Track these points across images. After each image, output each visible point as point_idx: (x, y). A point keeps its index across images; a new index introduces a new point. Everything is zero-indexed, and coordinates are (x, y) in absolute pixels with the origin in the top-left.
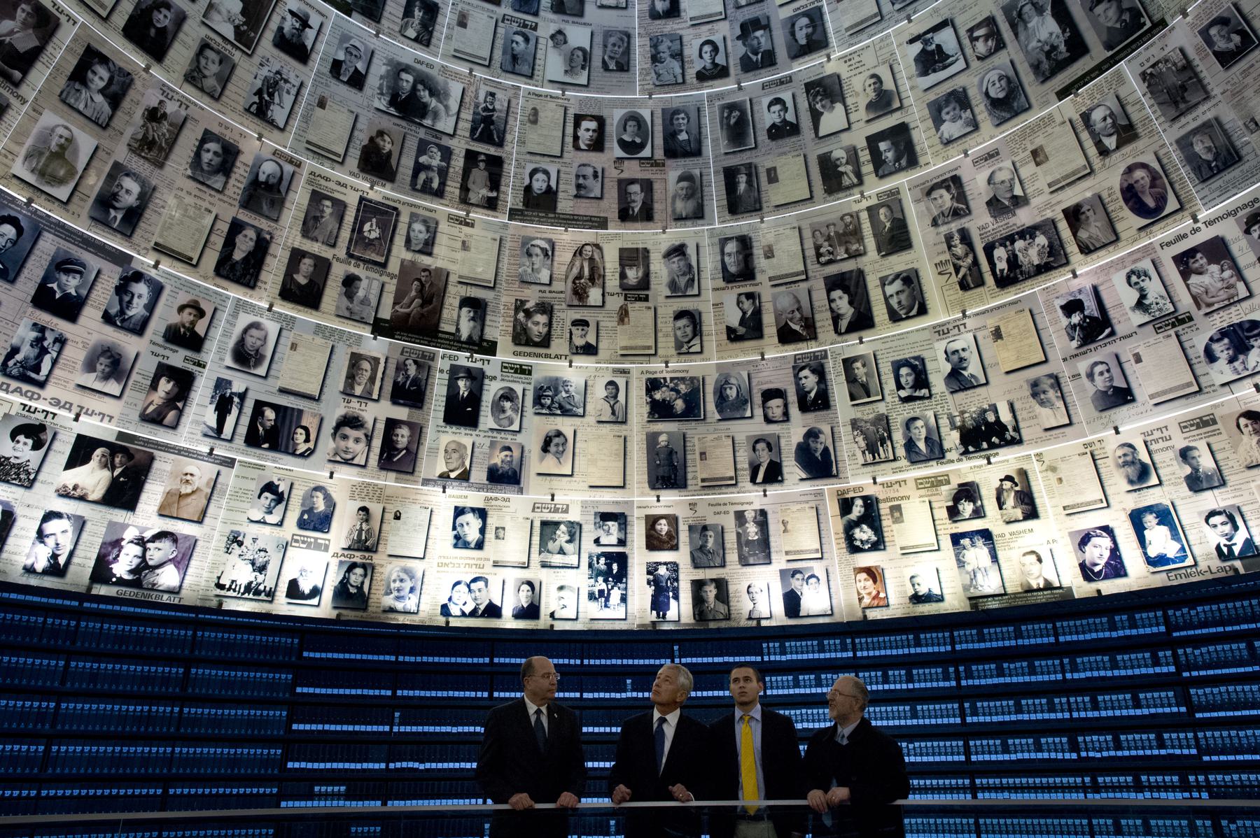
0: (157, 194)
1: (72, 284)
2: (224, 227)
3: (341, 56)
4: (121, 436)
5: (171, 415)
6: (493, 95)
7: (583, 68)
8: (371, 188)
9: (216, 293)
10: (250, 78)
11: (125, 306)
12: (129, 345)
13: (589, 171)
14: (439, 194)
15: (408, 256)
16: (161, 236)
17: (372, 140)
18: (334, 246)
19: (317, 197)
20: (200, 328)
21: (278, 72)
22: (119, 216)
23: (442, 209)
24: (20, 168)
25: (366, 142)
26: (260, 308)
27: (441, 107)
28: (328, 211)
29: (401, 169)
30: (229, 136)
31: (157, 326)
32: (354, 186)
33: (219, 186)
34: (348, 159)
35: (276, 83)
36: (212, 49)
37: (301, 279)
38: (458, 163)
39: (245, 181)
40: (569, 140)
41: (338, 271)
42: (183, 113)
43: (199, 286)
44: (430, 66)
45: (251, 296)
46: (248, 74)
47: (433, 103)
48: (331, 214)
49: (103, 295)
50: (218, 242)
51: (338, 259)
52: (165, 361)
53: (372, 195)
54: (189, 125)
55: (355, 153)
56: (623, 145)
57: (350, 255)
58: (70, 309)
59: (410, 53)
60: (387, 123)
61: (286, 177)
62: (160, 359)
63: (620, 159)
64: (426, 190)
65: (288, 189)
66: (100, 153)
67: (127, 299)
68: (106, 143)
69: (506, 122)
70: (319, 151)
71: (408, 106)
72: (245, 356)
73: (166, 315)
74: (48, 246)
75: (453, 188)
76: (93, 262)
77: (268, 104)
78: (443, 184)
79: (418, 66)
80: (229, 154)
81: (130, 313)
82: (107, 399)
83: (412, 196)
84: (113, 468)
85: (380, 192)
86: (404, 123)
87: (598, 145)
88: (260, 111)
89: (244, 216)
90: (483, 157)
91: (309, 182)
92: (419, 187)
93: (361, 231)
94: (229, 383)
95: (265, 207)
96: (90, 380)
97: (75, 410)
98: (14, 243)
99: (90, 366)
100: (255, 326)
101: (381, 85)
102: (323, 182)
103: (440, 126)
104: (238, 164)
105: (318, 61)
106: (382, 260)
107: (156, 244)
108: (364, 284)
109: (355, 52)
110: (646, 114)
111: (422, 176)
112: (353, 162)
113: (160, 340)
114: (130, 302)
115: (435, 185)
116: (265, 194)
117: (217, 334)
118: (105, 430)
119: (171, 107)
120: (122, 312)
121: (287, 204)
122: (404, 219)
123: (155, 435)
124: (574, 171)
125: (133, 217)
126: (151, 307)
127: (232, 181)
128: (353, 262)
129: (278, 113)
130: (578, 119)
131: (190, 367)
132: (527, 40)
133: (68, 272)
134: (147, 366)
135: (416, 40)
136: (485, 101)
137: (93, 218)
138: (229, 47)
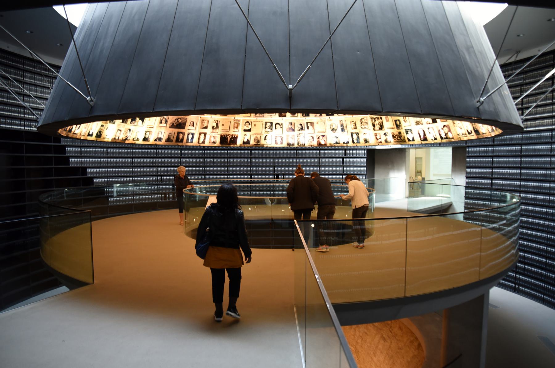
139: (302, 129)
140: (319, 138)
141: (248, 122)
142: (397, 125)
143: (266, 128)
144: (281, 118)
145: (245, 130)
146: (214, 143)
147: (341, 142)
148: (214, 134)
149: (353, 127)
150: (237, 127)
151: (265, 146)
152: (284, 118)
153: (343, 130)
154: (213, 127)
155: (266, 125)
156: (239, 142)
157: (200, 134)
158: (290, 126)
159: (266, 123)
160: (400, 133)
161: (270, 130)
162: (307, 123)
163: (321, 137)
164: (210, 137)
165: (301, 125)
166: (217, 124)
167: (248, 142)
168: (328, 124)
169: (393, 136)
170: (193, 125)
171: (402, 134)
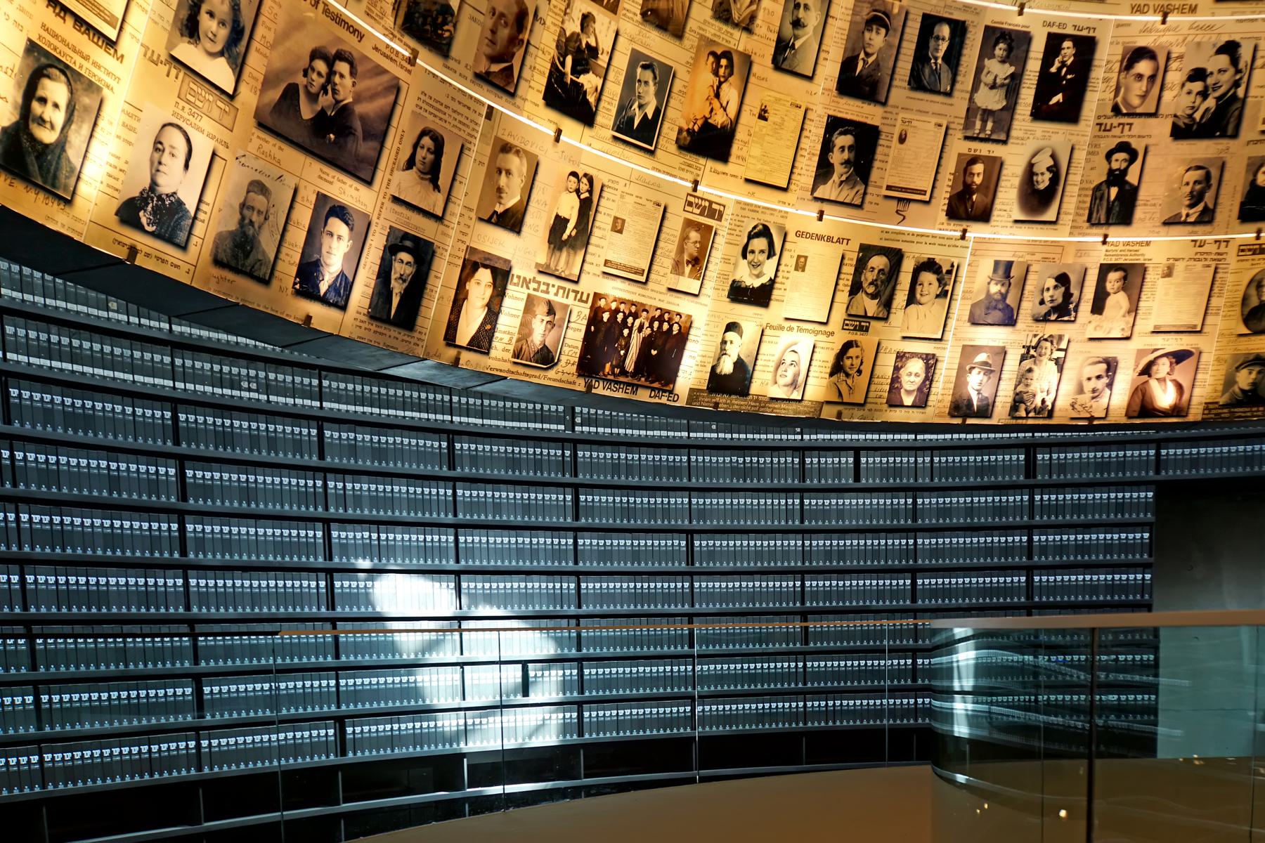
139: (1063, 310)
140: (1147, 371)
141: (765, 232)
143: (856, 288)
144: (953, 230)
145: (738, 293)
146: (546, 358)
148: (554, 292)
150: (696, 261)
152: (977, 231)
154: (557, 235)
155: (861, 265)
156: (691, 373)
157: (470, 267)
158: (995, 289)
159: (867, 251)
161: (872, 307)
162: (1105, 269)
165: (1063, 279)
166: (586, 207)
167: (743, 373)
170: (432, 174)
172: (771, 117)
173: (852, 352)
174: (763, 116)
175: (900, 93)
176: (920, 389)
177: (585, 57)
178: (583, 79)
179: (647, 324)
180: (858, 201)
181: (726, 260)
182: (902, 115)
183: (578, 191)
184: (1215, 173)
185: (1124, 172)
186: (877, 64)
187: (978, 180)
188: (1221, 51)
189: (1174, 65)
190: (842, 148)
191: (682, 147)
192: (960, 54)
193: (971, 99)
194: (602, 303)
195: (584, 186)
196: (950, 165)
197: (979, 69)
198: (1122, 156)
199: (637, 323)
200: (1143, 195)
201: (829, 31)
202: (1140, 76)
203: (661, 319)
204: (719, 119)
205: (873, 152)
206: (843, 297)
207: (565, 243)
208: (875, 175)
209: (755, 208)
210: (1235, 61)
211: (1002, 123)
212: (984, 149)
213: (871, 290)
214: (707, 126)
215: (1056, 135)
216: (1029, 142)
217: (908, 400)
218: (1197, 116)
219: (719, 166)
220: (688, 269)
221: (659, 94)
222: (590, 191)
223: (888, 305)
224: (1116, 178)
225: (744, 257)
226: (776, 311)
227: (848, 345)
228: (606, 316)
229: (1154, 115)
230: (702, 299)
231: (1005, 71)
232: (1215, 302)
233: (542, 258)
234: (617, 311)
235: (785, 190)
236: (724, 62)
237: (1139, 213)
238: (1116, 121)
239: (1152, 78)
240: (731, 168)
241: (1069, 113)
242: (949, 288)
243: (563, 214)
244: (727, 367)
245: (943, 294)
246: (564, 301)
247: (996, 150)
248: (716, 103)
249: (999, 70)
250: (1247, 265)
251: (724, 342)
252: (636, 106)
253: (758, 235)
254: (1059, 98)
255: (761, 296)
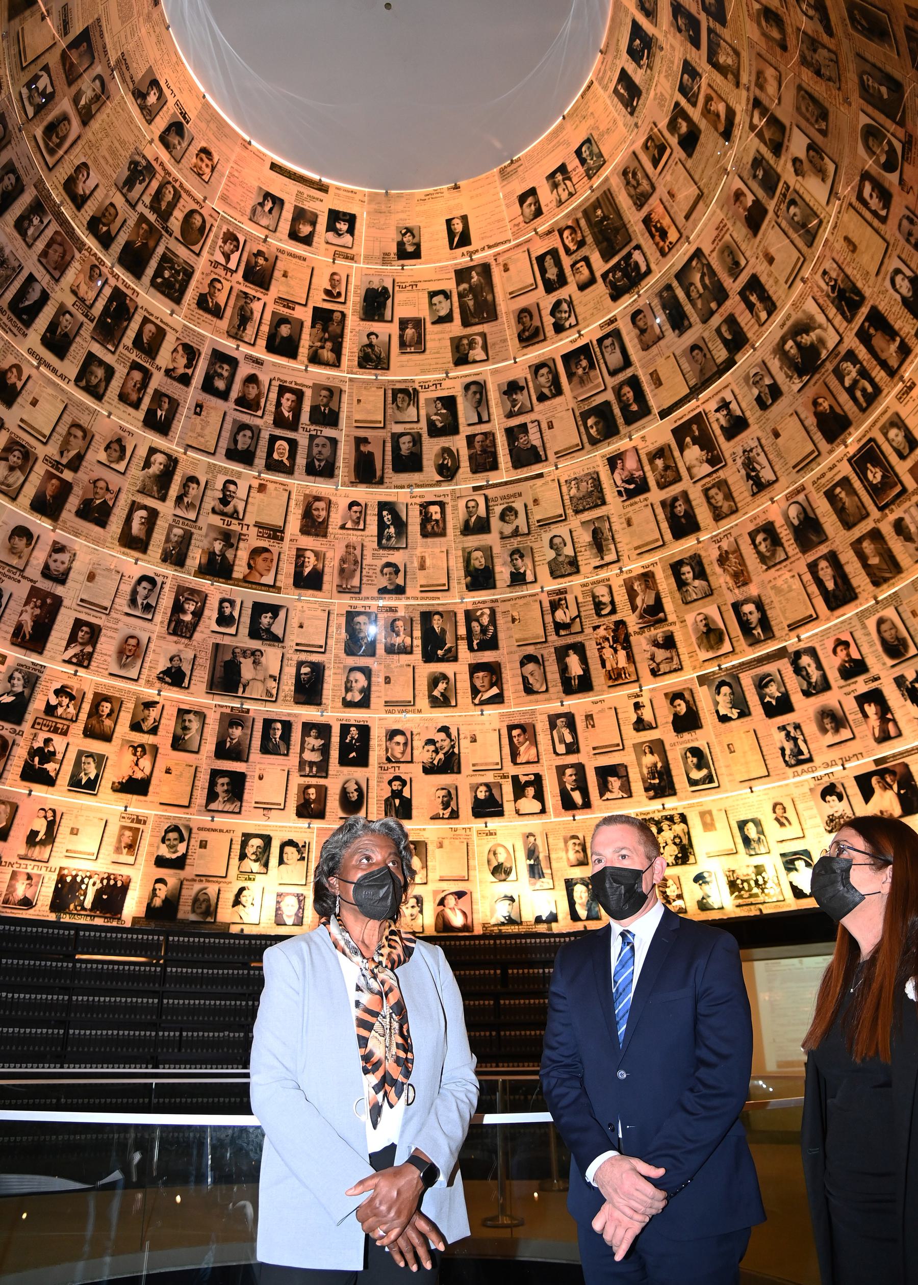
0: (763, 598)
1: (773, 690)
2: (808, 577)
3: (756, 392)
4: (877, 762)
5: (891, 726)
6: (825, 273)
7: (823, 159)
8: (846, 446)
9: (842, 622)
10: (738, 475)
11: (807, 677)
12: (829, 699)
13: (905, 223)
14: (878, 391)
15: (909, 463)
16: (786, 619)
17: (816, 414)
18: (868, 515)
19: (830, 495)
20: (855, 655)
21: (744, 451)
22: (759, 630)
23: (888, 402)
24: (704, 655)
25: (815, 421)
26: (872, 606)
27: (818, 331)
28: (843, 495)
29: (846, 408)
30: (760, 522)
31: (833, 676)
32: (837, 460)
33: (783, 557)
34: (819, 446)
35: (749, 458)
36: (710, 489)
37: (874, 561)
38: (862, 353)
39: (791, 536)
40: (876, 223)
41: (887, 529)
42: (732, 539)
43: (829, 628)
44: (789, 316)
45: (861, 605)
46: (733, 474)
47: (813, 335)
48: (847, 495)
49: (794, 684)
50: (813, 589)
51: (878, 521)
52: (857, 694)
53: (852, 450)
54: (740, 542)
55: (818, 436)
56: (889, 166)
57: (881, 509)
58: (783, 706)
59: (774, 329)
60: (810, 392)
61: (805, 504)
62: (853, 695)
63: (901, 181)
64: (872, 398)
65: (813, 510)
66: (723, 608)
67: (804, 673)
68: (720, 601)
69: (847, 276)
70: (803, 465)
71: (806, 362)
72: (895, 649)
73: (832, 664)
74: (747, 680)
75: (879, 375)
76: (770, 668)
77: (757, 476)
78: (872, 381)
79: (786, 328)
80: (769, 530)
81: (813, 680)
82: (849, 743)
83: (871, 415)
84: (891, 787)
85: (853, 441)
86: (817, 376)
87: (885, 196)
88: (759, 486)
89: (811, 557)
90: (867, 324)
91: (818, 490)
92: (864, 405)
93: (870, 483)
94: (902, 676)
95: (814, 538)
96: (830, 738)
97: (840, 762)
98: (733, 693)
99: (824, 731)
100: (881, 622)
101: (786, 373)
102: (823, 481)
103: (831, 345)
104: (779, 531)
105: (752, 414)
106: (899, 488)
107: (789, 626)
108: (908, 520)
109: (757, 378)
110: (864, 120)
111: (858, 394)
112: (823, 445)
113: (842, 682)
114: (808, 674)
115: (870, 389)
116: (808, 530)
117: (865, 650)
118: (865, 764)
119: (725, 545)
120: (809, 684)
121: (822, 520)
122: (881, 439)
123: (894, 748)
124: (902, 241)
125: (765, 623)
126: (820, 667)
127: (786, 545)
128: (887, 511)
129: (767, 475)
130: (860, 198)
131: (873, 685)
132: (793, 202)
133: (766, 685)
134: (851, 706)
135: (769, 314)
136: (827, 284)
137: (750, 645)
138: (714, 476)
140: (442, 902)
142: (747, 841)
143: (243, 856)
144: (303, 823)
145: (160, 862)
147: (528, 916)
149: (573, 856)
151: (234, 929)
153: (535, 871)
154: (32, 839)
155: (244, 844)
156: (133, 906)
159: (247, 837)
160: (759, 870)
161: (256, 867)
163: (451, 901)
164: (14, 875)
166: (52, 826)
168: (480, 848)
169: (733, 885)
171: (769, 874)
172: (174, 772)
173: (245, 893)
174: (168, 771)
175: (255, 755)
176: (296, 915)
177: (48, 757)
178: (45, 766)
179: (98, 881)
180: (237, 810)
181: (151, 845)
182: (258, 766)
183: (45, 817)
184: (453, 792)
185: (401, 791)
186: (239, 743)
187: (313, 797)
188: (440, 730)
189: (415, 738)
190: (223, 785)
191: (115, 790)
192: (289, 736)
193: (300, 757)
194: (66, 872)
195: (50, 814)
196: (294, 790)
197: (303, 742)
198: (397, 783)
199: (92, 881)
200: (414, 803)
201: (205, 730)
202: (398, 743)
203: (108, 879)
204: (139, 775)
205: (243, 785)
206: (235, 861)
207: (38, 843)
208: (246, 796)
209: (168, 818)
210: (449, 735)
211: (322, 768)
212: (313, 781)
213: (254, 857)
214: (131, 779)
215: (358, 773)
216: (339, 777)
217: (290, 921)
218: (436, 762)
219: (142, 798)
220: (125, 851)
221: (98, 767)
222: (54, 816)
223: (266, 865)
224: (397, 794)
225: (163, 841)
226: (189, 872)
227: (242, 890)
228: (69, 879)
229: (412, 762)
230: (136, 866)
231: (318, 743)
232: (471, 862)
233: (22, 852)
234: (77, 875)
235: (188, 807)
236: (139, 749)
237: (414, 813)
238: (390, 765)
239: (405, 744)
240: (149, 797)
241: (362, 761)
242: (305, 855)
243: (35, 829)
244: (158, 902)
245: (303, 859)
246: (39, 872)
247: (321, 782)
248: (136, 768)
249: (313, 742)
250: (484, 841)
251: (154, 890)
252: (82, 774)
253: (172, 831)
254: (354, 754)
255: (179, 863)
